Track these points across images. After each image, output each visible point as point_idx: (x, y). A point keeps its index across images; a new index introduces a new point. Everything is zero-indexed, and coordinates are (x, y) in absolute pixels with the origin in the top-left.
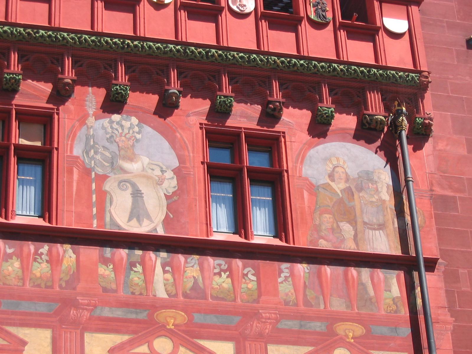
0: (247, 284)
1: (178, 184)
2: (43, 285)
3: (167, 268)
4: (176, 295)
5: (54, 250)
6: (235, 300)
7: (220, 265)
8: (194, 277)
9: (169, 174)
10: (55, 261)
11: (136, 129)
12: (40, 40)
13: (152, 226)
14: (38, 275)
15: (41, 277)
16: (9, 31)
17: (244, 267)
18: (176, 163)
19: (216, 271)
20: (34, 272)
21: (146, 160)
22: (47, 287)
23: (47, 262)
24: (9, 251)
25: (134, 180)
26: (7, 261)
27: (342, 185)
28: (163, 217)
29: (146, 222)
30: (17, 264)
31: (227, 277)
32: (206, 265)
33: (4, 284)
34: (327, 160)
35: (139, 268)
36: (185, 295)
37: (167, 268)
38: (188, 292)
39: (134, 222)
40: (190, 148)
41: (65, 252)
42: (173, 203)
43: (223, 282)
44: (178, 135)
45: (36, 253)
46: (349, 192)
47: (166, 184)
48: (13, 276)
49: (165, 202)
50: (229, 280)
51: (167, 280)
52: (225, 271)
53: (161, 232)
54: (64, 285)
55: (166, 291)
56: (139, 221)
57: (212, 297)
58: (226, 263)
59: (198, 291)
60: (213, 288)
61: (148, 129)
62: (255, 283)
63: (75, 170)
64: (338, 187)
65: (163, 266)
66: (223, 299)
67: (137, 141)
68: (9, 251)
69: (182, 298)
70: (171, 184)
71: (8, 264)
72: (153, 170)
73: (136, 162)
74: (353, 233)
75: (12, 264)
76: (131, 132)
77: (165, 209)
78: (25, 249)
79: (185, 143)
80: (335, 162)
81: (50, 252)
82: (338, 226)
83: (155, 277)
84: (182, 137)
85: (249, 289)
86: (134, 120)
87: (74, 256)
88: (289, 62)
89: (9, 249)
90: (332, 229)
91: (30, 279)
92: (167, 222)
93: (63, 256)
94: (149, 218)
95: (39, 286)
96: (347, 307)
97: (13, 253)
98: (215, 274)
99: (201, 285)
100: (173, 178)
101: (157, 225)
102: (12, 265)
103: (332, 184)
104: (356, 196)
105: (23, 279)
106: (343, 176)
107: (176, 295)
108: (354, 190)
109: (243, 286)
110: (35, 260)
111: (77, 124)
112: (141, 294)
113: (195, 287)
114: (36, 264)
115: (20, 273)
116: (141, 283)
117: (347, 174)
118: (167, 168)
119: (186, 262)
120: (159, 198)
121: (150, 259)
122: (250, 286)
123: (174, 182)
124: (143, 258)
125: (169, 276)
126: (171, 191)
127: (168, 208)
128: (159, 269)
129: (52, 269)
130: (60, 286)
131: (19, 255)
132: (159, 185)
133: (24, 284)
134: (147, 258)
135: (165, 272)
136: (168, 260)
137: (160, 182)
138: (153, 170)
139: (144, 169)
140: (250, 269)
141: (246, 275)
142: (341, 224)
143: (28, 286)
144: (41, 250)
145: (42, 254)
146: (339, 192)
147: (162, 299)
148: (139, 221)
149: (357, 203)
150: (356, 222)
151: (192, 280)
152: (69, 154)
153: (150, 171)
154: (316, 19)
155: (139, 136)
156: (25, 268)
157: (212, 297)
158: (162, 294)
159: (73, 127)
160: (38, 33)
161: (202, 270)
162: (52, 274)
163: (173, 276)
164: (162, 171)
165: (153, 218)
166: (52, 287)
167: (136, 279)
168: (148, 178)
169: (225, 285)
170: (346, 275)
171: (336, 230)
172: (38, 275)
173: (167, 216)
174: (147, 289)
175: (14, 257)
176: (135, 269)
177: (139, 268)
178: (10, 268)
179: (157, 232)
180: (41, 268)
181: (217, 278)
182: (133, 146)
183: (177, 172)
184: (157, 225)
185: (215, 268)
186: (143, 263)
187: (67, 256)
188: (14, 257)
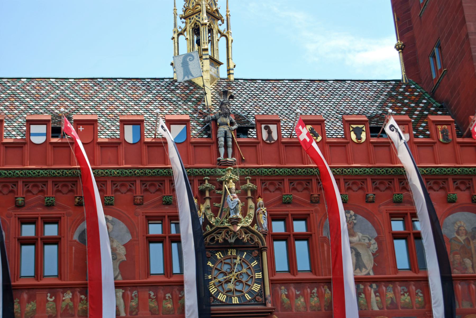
0: (418, 298)
1: (378, 246)
2: (316, 310)
3: (377, 294)
4: (383, 309)
5: (320, 290)
6: (413, 308)
7: (403, 289)
8: (391, 298)
9: (373, 241)
10: (321, 296)
11: (354, 217)
12: (300, 174)
13: (367, 272)
14: (313, 304)
15: (315, 306)
16: (283, 171)
17: (416, 289)
18: (376, 235)
19: (402, 293)
20: (311, 303)
21: (360, 235)
22: (319, 310)
23: (317, 297)
24: (298, 293)
25: (355, 247)
26: (297, 299)
27: (464, 237)
28: (372, 266)
29: (364, 270)
30: (302, 300)
31: (408, 295)
32: (396, 291)
33: (297, 311)
34: (454, 223)
35: (363, 296)
36: (388, 308)
37: (377, 294)
38: (389, 306)
39: (358, 270)
40: (382, 224)
41: (325, 290)
42: (377, 256)
43: (406, 298)
44: (375, 218)
45: (311, 293)
46: (467, 240)
47: (372, 247)
48: (301, 306)
49: (372, 257)
50: (409, 297)
51: (377, 300)
52: (406, 293)
53: (372, 274)
54: (327, 308)
55: (378, 306)
56: (361, 270)
57: (402, 308)
58: (407, 288)
59: (394, 305)
60: (401, 303)
61: (360, 217)
62: (422, 298)
63: (325, 244)
64: (462, 239)
65: (375, 293)
66: (407, 308)
67: (355, 224)
68: (298, 293)
69: (386, 310)
70: (374, 247)
71: (298, 300)
72: (364, 240)
73: (355, 236)
74: (471, 264)
75: (300, 299)
76: (351, 219)
77: (373, 261)
78: (305, 291)
79: (379, 222)
80: (459, 224)
81: (318, 291)
82: (463, 261)
83: (372, 300)
84: (378, 219)
85: (420, 301)
86: (352, 213)
87: (329, 292)
88: (431, 170)
89: (298, 291)
90: (460, 263)
91: (310, 307)
92: (375, 269)
93: (325, 293)
94: (365, 267)
95: (314, 310)
96: (471, 306)
97: (300, 294)
98: (402, 295)
99: (395, 301)
100: (375, 243)
101: (370, 271)
102: (300, 301)
103: (459, 237)
104: (471, 243)
105: (306, 307)
106: (464, 231)
107: (383, 309)
108: (470, 239)
109: (417, 300)
110: (311, 296)
111: (323, 218)
112: (365, 309)
113: (392, 303)
114: (312, 299)
115: (304, 304)
116: (365, 303)
117: (465, 230)
118: (372, 238)
119: (386, 290)
120: (369, 256)
121: (368, 290)
122: (420, 299)
123: (376, 246)
124: (364, 289)
125: (378, 298)
126: (375, 250)
127: (375, 261)
128: (373, 295)
129: (320, 301)
130: (325, 309)
131: (303, 295)
132: (369, 248)
133: (307, 310)
134: (366, 290)
135: (376, 296)
136: (377, 289)
137: (369, 246)
138: (364, 240)
139: (360, 240)
140: (419, 290)
141: (417, 294)
142: (465, 259)
143: (309, 311)
144: (313, 291)
145: (314, 293)
146: (462, 241)
147: (376, 311)
148: (361, 270)
149: (472, 246)
150: (472, 258)
151: (390, 299)
152: (321, 236)
153: (363, 241)
154: (443, 141)
155: (355, 221)
156: (306, 301)
157: (402, 308)
158: (376, 308)
159: (321, 220)
160: (298, 170)
161: (395, 293)
162: (320, 303)
163: (380, 297)
164: (369, 240)
165: (367, 267)
166: (321, 310)
167: (362, 301)
168: (362, 245)
169: (407, 300)
170: (469, 288)
171: (462, 263)
172: (313, 304)
173: (374, 265)
174: (368, 306)
175: (301, 296)
176: (361, 296)
177: (363, 296)
178: (299, 302)
179: (370, 275)
180: (314, 301)
181: (402, 297)
182: (353, 228)
183: (377, 239)
184: (370, 271)
185: (401, 291)
186: (364, 293)
187: (326, 293)
188: (301, 296)
